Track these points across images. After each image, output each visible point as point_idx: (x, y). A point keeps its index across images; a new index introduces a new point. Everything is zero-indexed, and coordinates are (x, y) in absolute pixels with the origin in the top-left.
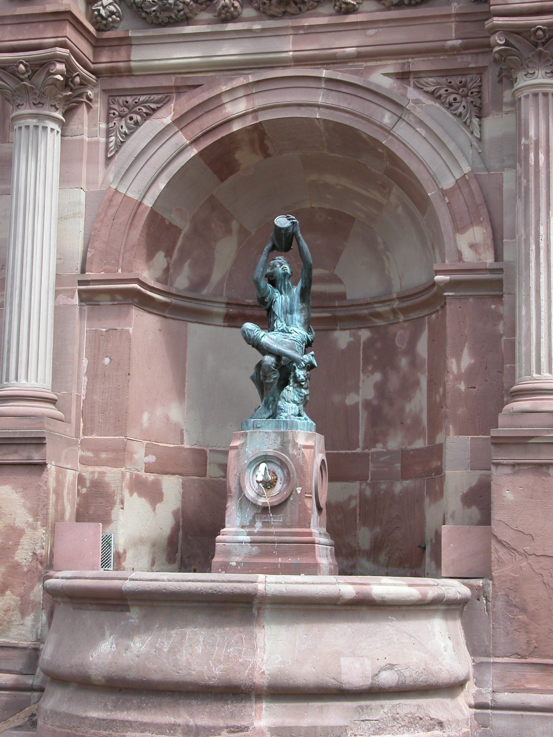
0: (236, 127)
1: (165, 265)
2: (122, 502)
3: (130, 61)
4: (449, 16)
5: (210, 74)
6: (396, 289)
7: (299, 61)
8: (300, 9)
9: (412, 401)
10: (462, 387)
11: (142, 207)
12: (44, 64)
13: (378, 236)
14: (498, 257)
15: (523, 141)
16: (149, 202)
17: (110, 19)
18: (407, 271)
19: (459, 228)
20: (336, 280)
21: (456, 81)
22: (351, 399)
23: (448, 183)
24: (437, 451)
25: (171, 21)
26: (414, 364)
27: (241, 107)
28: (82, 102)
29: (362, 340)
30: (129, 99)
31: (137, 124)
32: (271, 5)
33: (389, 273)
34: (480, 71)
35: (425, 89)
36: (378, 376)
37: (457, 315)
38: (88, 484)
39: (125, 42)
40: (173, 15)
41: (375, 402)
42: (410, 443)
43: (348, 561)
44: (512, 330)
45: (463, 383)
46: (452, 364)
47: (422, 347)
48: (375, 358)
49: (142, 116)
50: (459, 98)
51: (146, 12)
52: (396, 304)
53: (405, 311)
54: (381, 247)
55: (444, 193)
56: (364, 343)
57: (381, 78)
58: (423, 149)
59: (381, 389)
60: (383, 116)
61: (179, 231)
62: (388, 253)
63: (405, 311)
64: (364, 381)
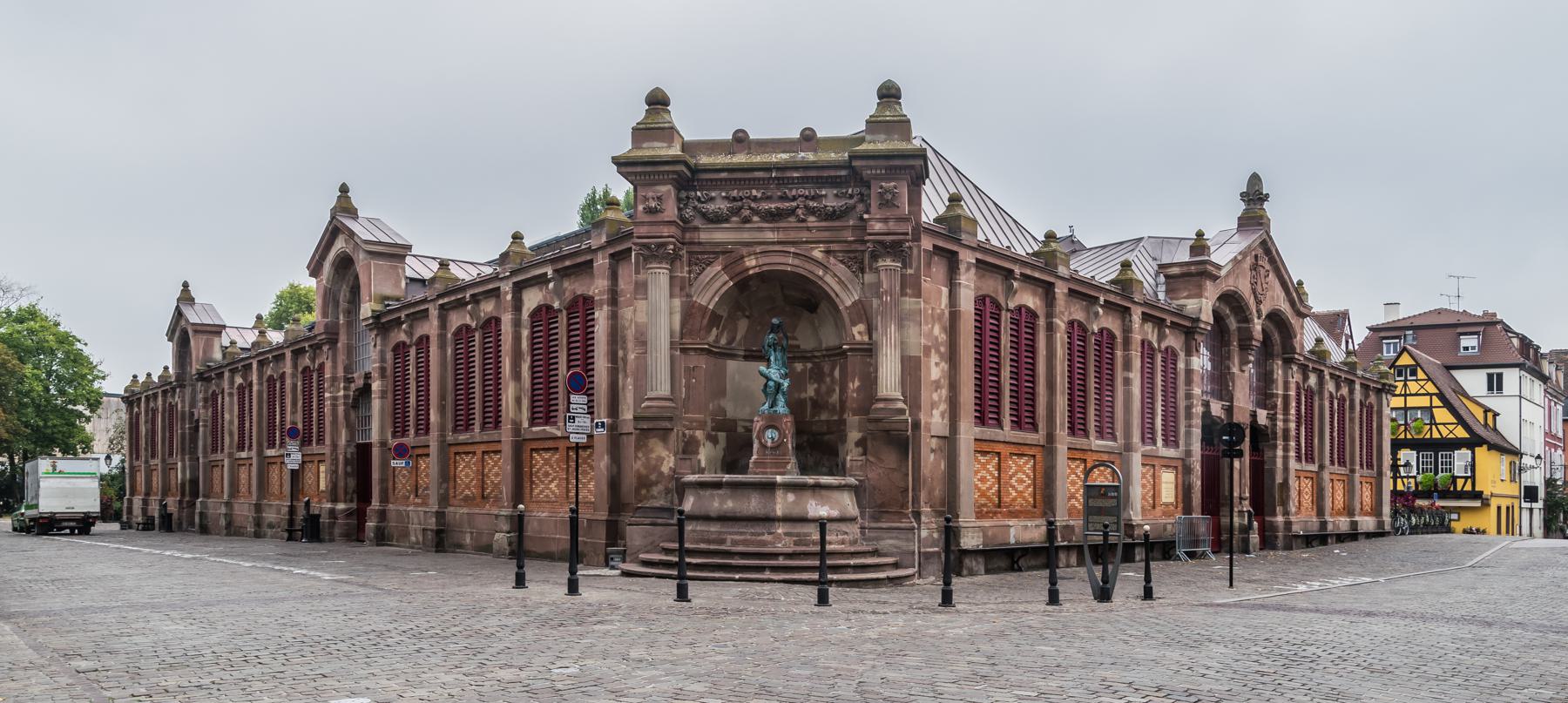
7: (779, 243)
12: (664, 245)
14: (870, 338)
18: (829, 339)
19: (854, 324)
20: (795, 338)
22: (803, 395)
23: (849, 303)
24: (842, 422)
37: (854, 361)
39: (696, 229)
43: (804, 470)
44: (876, 371)
47: (837, 373)
57: (817, 254)
58: (837, 288)
59: (817, 391)
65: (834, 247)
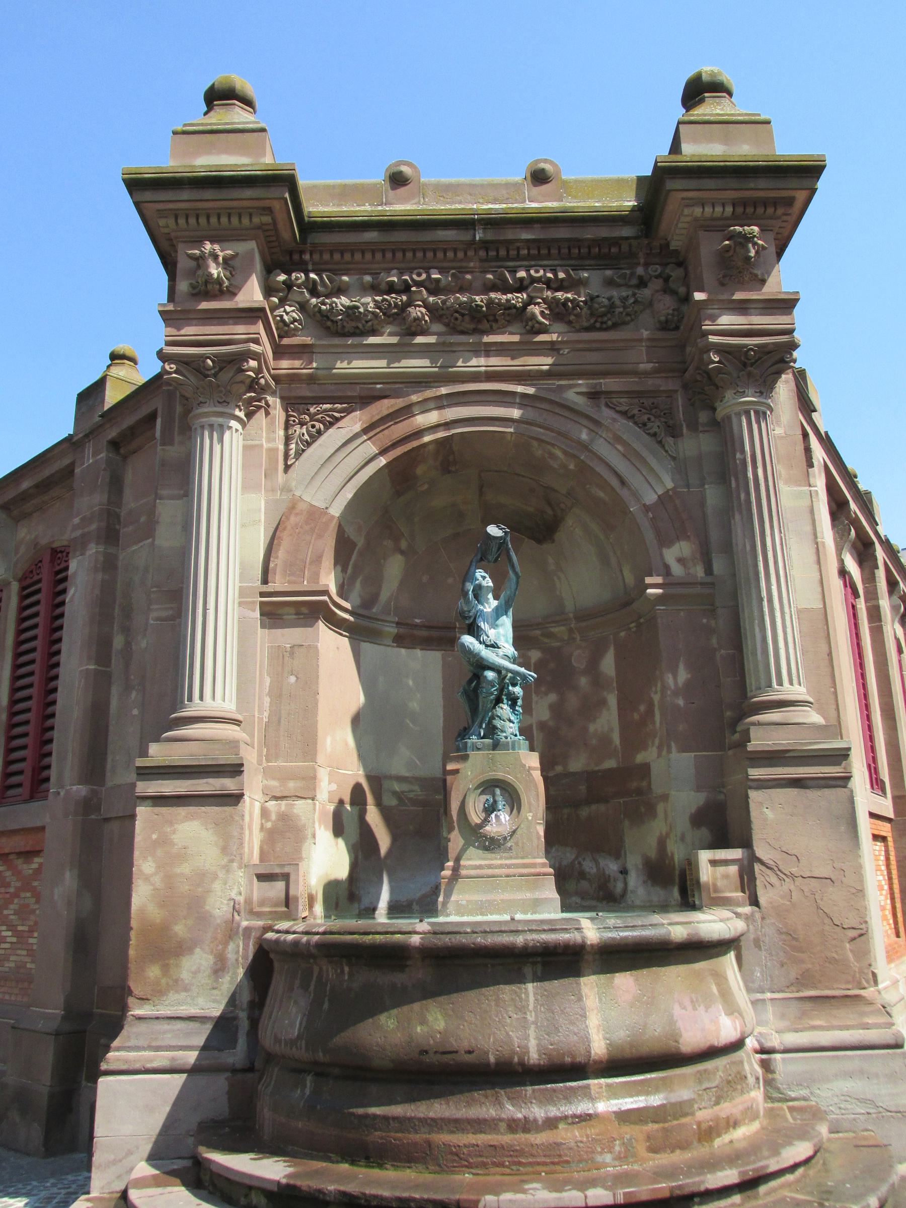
0: (427, 439)
2: (314, 836)
4: (641, 340)
5: (397, 386)
7: (491, 376)
8: (491, 327)
10: (681, 702)
14: (709, 571)
15: (738, 456)
16: (336, 511)
17: (292, 326)
19: (665, 541)
21: (648, 402)
23: (650, 498)
25: (358, 331)
27: (433, 417)
28: (262, 407)
31: (320, 433)
32: (463, 321)
34: (670, 394)
35: (618, 408)
38: (274, 817)
40: (360, 326)
45: (681, 698)
46: (670, 680)
49: (324, 425)
50: (653, 419)
51: (332, 321)
55: (647, 508)
60: (581, 432)
65: (608, 384)
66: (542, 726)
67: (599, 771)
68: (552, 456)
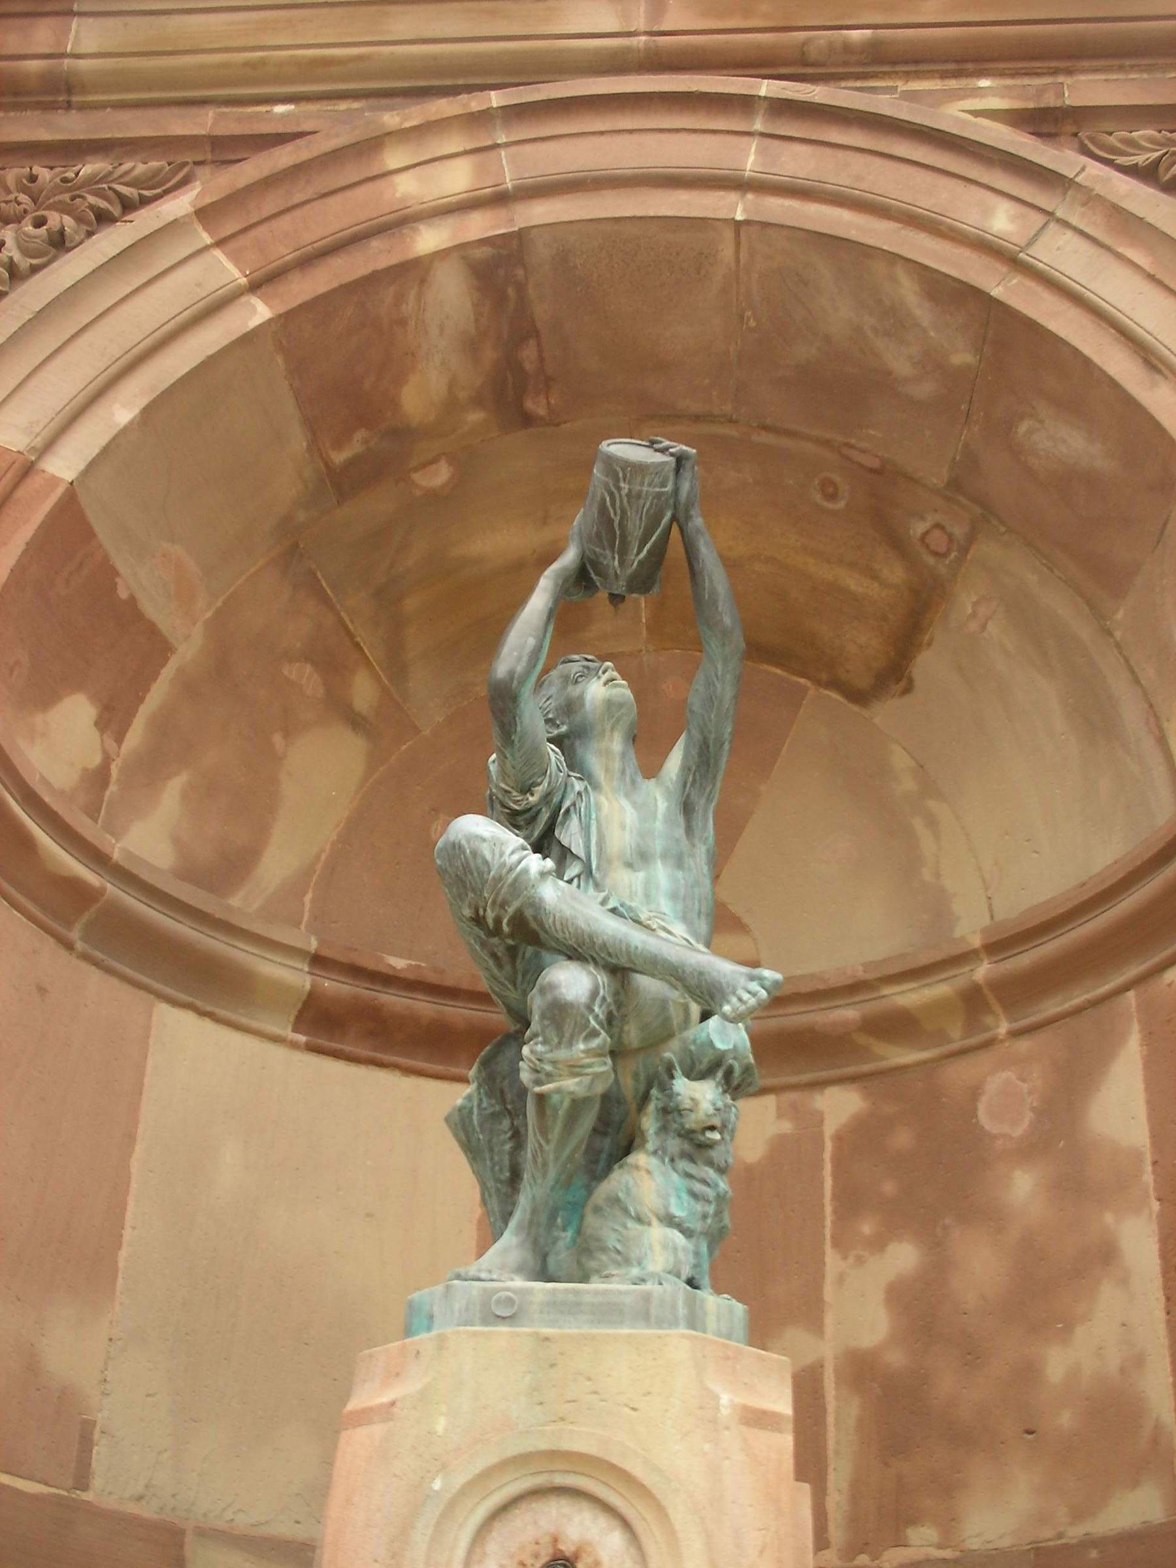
1: (97, 760)
3: (63, 55)
6: (970, 929)
9: (1080, 1331)
11: (34, 483)
13: (896, 748)
16: (64, 465)
26: (1080, 1178)
29: (829, 1129)
30: (44, 174)
33: (938, 876)
36: (903, 1257)
41: (895, 1358)
42: (1078, 1515)
48: (889, 1188)
49: (79, 220)
52: (982, 971)
53: (1017, 992)
54: (908, 784)
56: (838, 1138)
60: (987, 212)
61: (161, 648)
62: (931, 804)
63: (1017, 992)
64: (841, 1279)
66: (860, 1369)
67: (1090, 1542)
68: (895, 321)
